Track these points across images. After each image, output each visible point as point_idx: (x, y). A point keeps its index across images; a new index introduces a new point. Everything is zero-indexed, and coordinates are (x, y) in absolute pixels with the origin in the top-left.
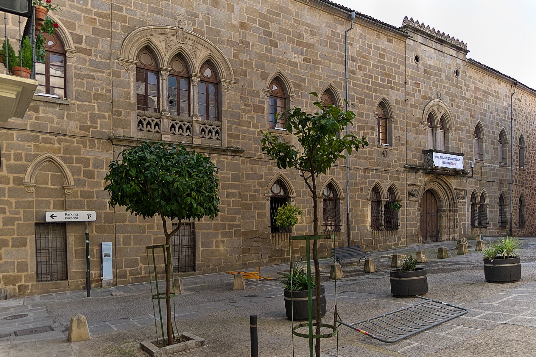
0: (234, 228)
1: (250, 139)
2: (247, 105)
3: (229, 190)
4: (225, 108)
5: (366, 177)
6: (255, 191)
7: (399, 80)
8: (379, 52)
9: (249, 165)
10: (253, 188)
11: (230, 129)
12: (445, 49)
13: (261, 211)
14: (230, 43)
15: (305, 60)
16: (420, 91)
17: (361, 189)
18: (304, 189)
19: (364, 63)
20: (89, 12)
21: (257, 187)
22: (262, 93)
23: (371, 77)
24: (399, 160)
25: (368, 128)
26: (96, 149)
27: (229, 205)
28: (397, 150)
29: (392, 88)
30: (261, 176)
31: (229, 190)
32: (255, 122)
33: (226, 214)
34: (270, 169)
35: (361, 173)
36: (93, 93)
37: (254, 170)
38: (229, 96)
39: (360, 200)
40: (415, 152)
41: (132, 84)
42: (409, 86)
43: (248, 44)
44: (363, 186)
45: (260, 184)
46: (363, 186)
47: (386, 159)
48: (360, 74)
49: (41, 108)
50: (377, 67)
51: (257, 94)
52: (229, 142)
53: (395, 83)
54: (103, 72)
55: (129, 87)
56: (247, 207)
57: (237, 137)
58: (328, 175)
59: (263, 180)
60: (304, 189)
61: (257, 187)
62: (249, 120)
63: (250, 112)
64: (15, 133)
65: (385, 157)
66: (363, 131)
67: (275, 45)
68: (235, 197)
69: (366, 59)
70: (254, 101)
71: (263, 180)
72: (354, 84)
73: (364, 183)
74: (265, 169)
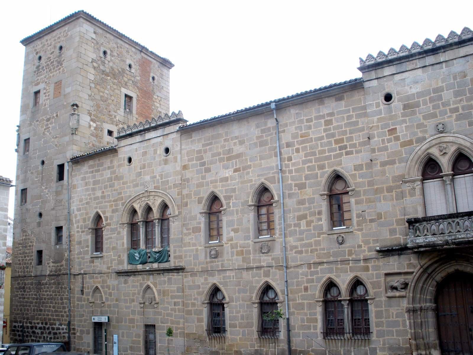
0: (179, 330)
1: (190, 256)
2: (187, 229)
3: (176, 300)
4: (172, 236)
5: (312, 274)
6: (195, 300)
7: (358, 138)
8: (323, 121)
9: (190, 278)
10: (193, 297)
11: (175, 252)
12: (442, 57)
13: (199, 316)
14: (175, 186)
15: (236, 171)
16: (397, 138)
17: (306, 289)
18: (237, 294)
19: (303, 142)
20: (110, 201)
21: (196, 296)
22: (199, 216)
23: (314, 154)
24: (366, 242)
25: (313, 214)
26: (112, 280)
27: (175, 312)
28: (361, 230)
29: (347, 153)
30: (199, 287)
31: (176, 300)
32: (194, 241)
33: (173, 318)
34: (206, 279)
35: (305, 269)
36: (111, 247)
37: (193, 282)
38: (174, 226)
39: (305, 302)
40: (395, 226)
41: (125, 236)
42: (376, 139)
43: (188, 180)
44: (309, 285)
45: (199, 294)
46: (309, 285)
47: (343, 245)
48: (298, 158)
49: (95, 261)
50: (322, 138)
51: (195, 218)
52: (175, 263)
53: (354, 146)
54: (115, 234)
55: (123, 239)
56: (189, 312)
57: (180, 257)
58: (262, 278)
59: (201, 290)
60: (237, 294)
61: (196, 296)
62: (189, 241)
63: (190, 234)
64: (87, 275)
65: (341, 244)
66: (305, 221)
67: (208, 170)
68: (179, 305)
69: (305, 137)
70: (194, 224)
71: (201, 290)
72: (290, 172)
73: (308, 281)
74: (202, 280)
